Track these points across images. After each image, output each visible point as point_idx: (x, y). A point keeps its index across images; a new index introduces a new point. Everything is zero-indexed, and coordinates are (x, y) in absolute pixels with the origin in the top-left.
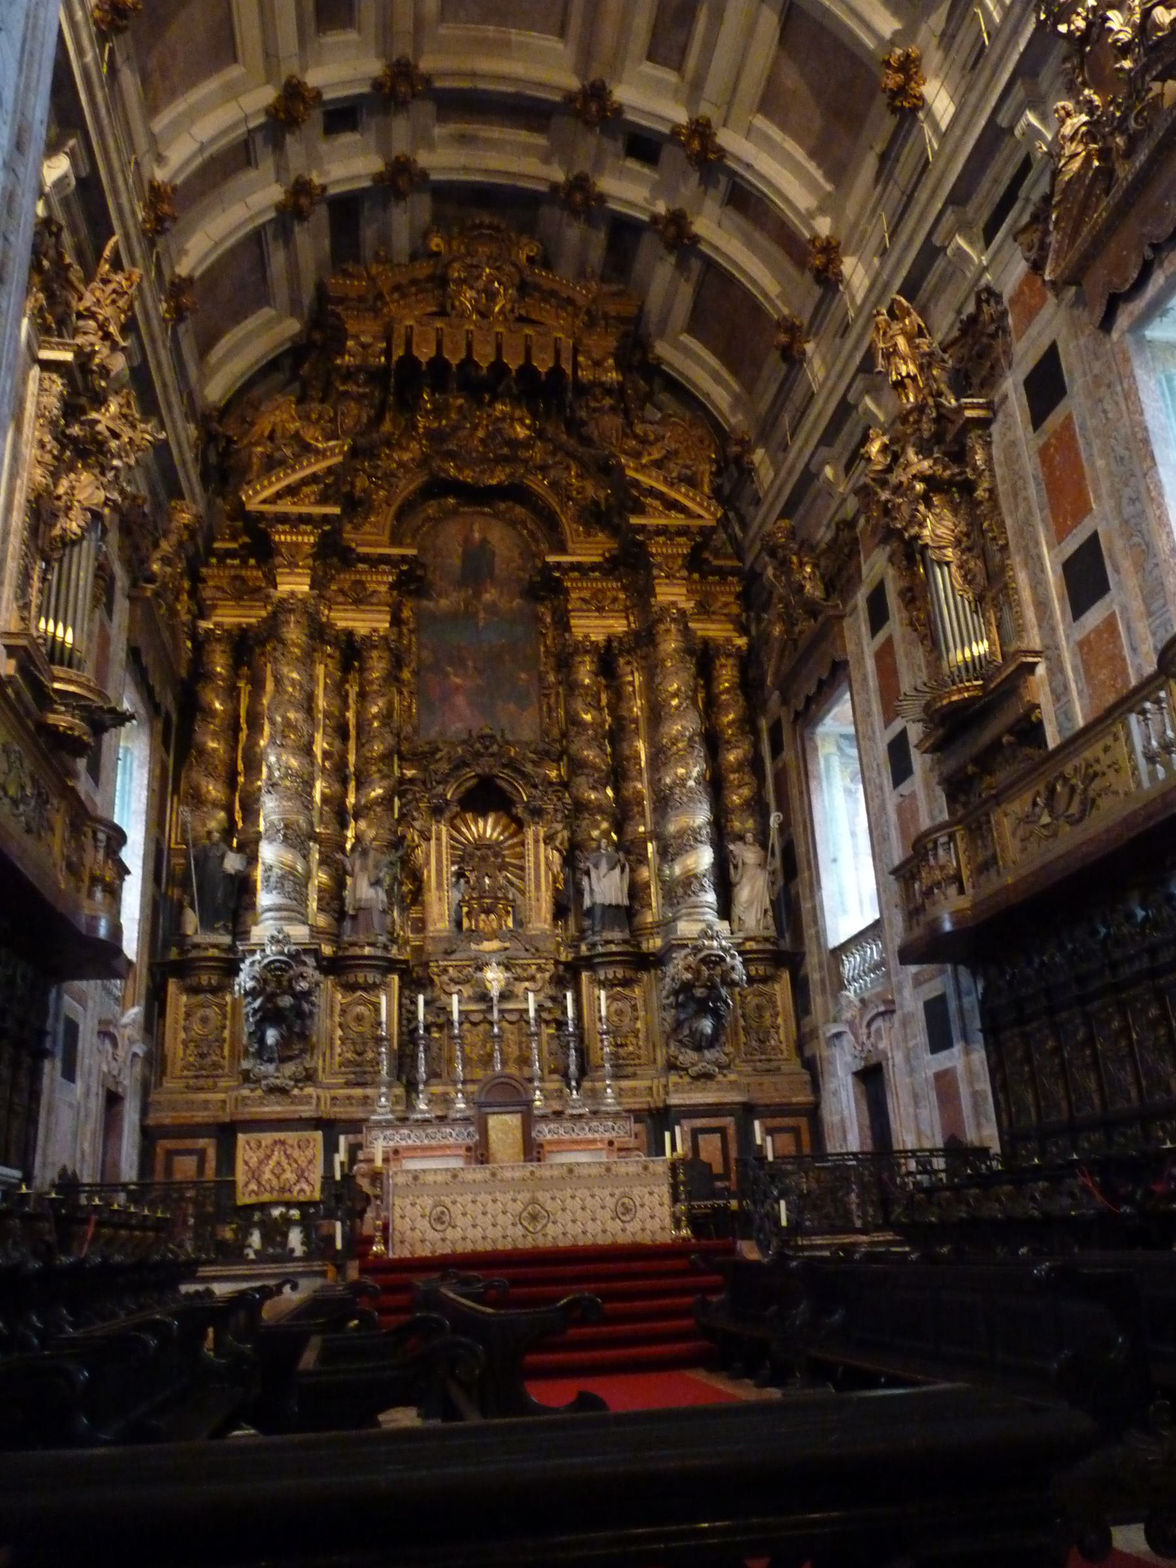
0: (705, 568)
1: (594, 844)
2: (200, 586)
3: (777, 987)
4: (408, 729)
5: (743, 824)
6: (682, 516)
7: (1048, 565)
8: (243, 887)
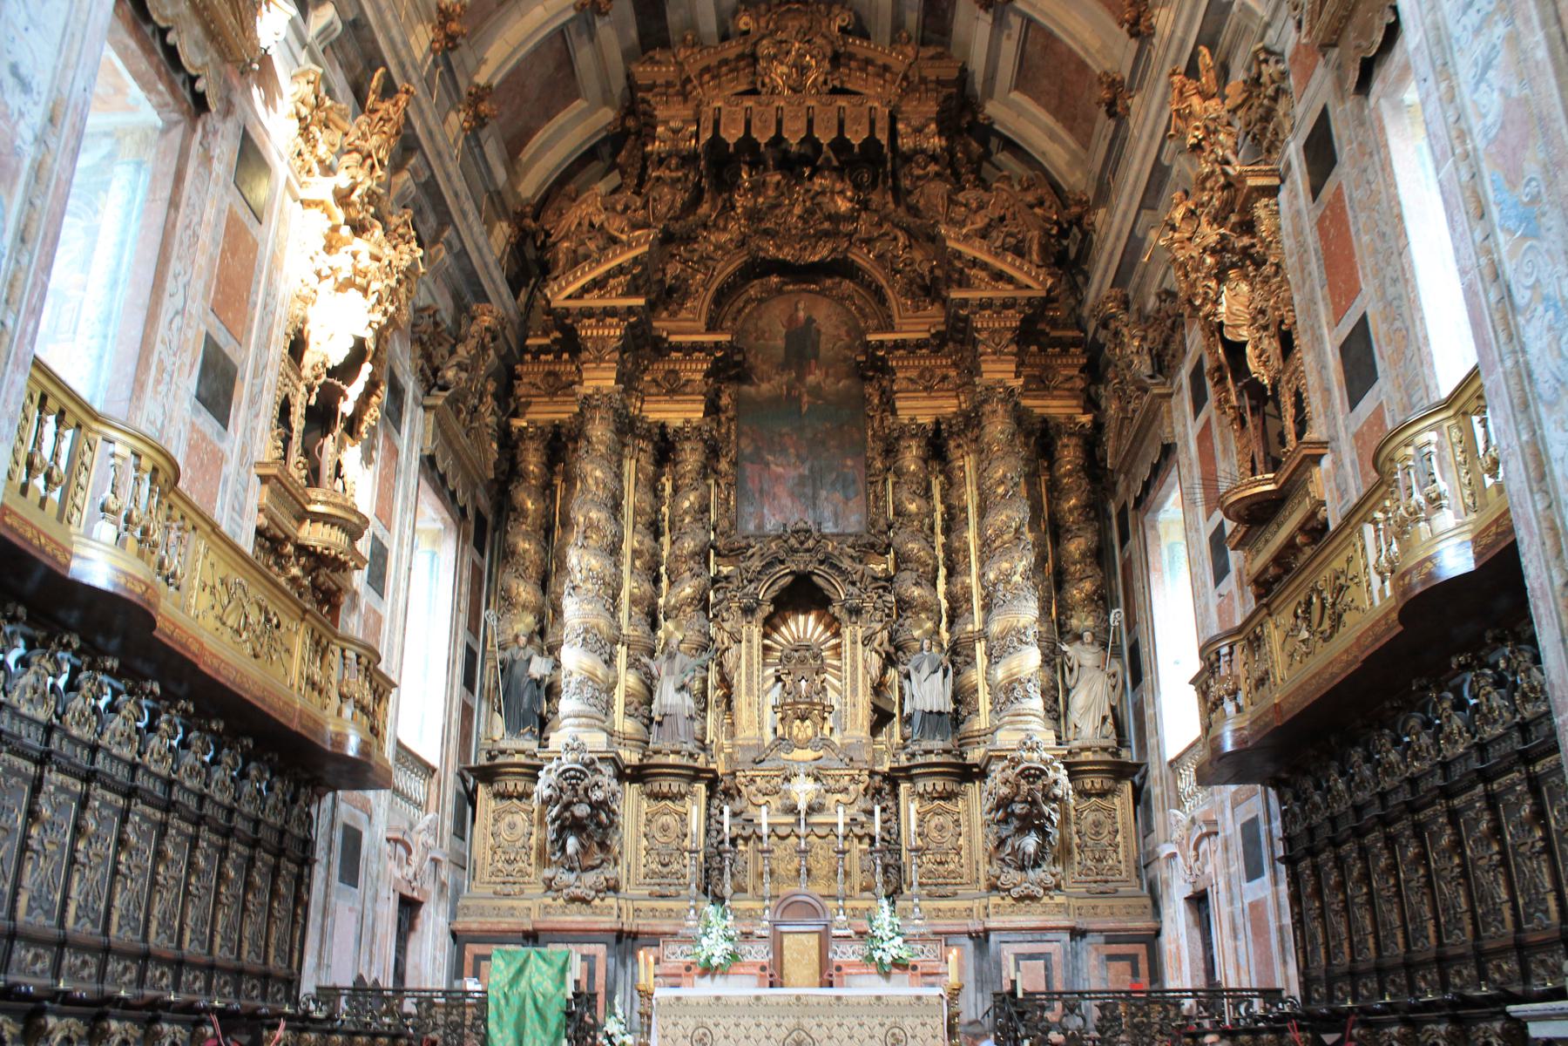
0: (1042, 339)
1: (917, 645)
2: (516, 383)
3: (1116, 800)
4: (724, 524)
5: (1082, 621)
6: (1011, 287)
7: (1328, 347)
8: (551, 691)
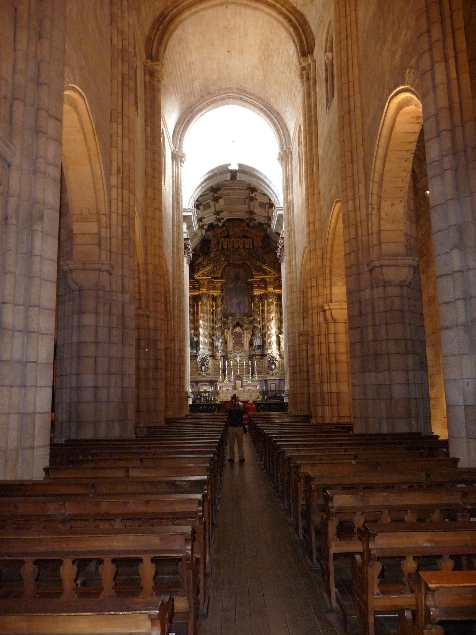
8: (198, 343)
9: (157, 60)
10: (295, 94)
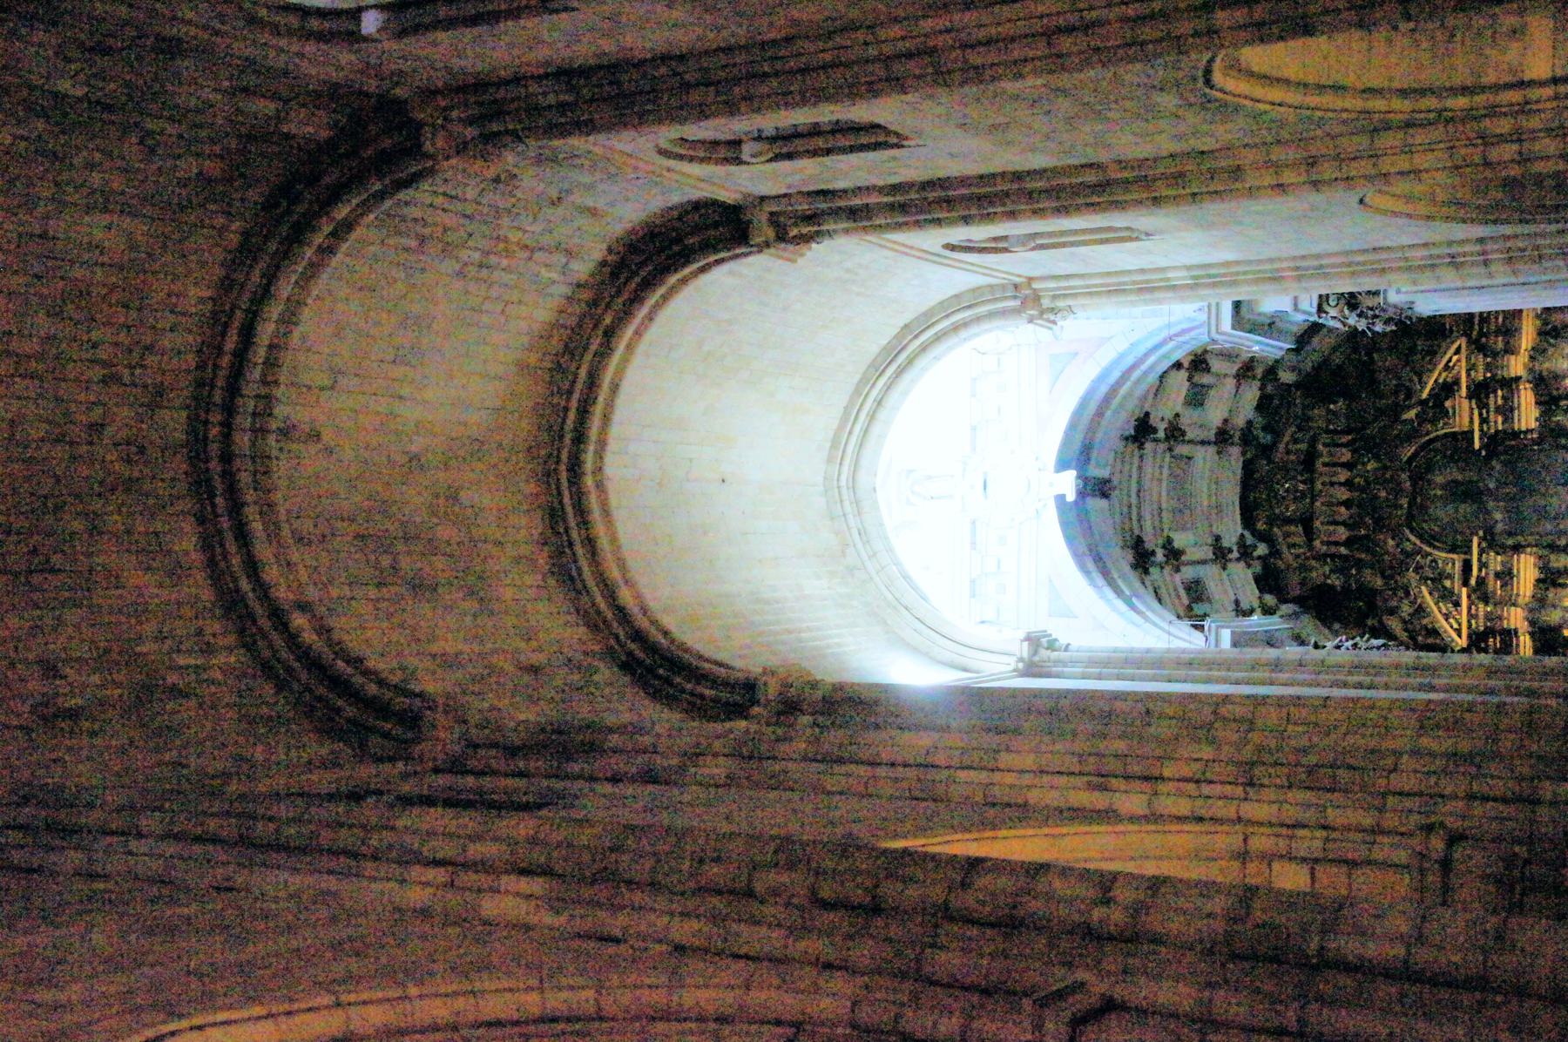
9: (750, 687)
10: (848, 271)
